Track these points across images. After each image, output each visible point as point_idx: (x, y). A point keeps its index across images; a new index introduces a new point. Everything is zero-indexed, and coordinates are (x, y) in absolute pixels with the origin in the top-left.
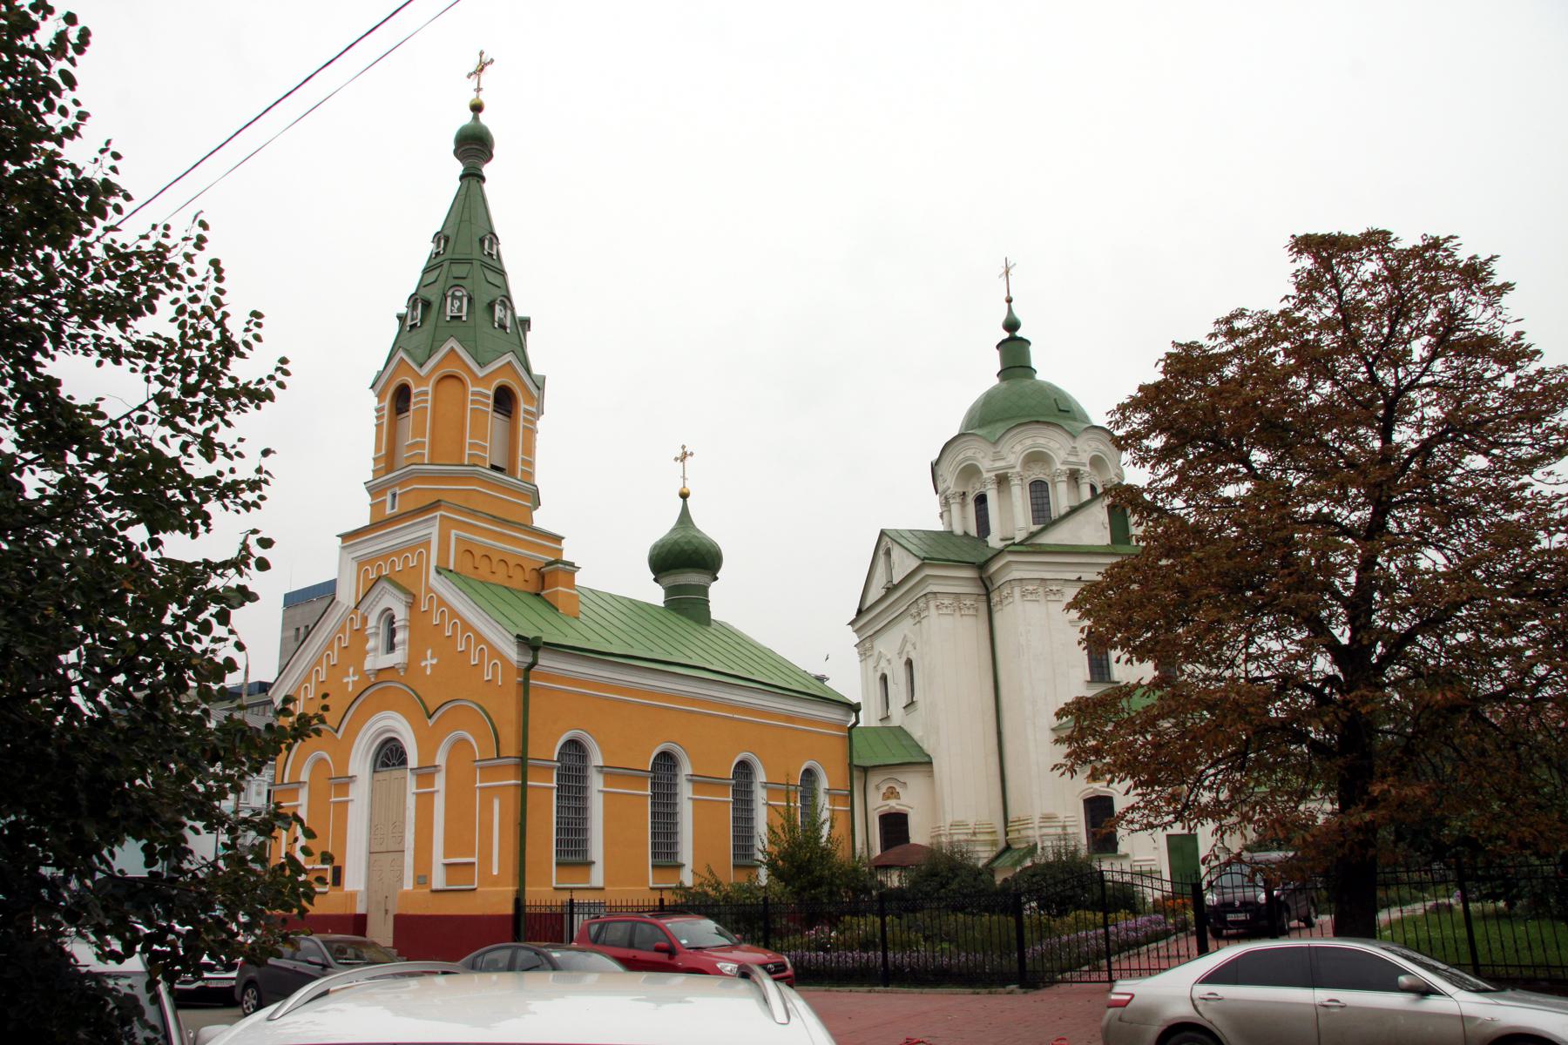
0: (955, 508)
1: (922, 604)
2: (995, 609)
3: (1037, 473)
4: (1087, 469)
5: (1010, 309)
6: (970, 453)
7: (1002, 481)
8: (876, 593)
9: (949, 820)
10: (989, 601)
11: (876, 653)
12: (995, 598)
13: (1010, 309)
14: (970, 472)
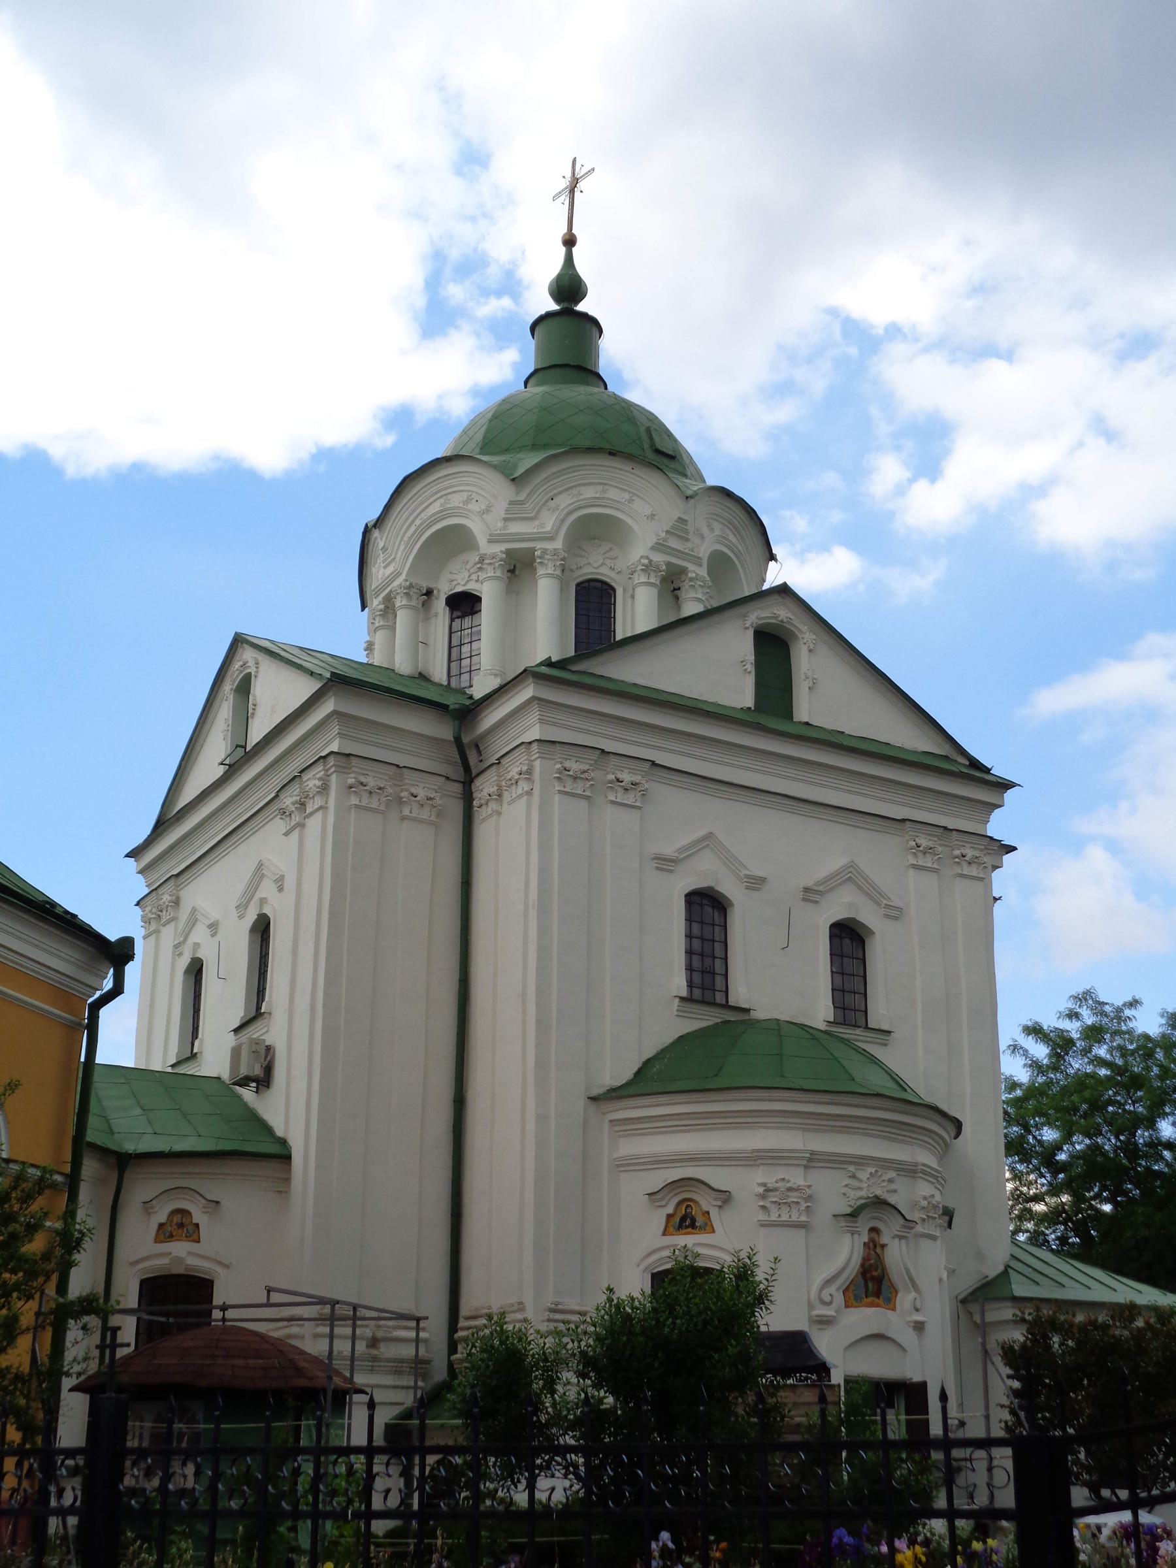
0: (403, 618)
1: (312, 781)
2: (480, 814)
4: (703, 572)
5: (569, 260)
6: (456, 500)
7: (518, 568)
8: (208, 769)
10: (468, 799)
11: (184, 914)
12: (485, 787)
13: (569, 260)
14: (449, 542)
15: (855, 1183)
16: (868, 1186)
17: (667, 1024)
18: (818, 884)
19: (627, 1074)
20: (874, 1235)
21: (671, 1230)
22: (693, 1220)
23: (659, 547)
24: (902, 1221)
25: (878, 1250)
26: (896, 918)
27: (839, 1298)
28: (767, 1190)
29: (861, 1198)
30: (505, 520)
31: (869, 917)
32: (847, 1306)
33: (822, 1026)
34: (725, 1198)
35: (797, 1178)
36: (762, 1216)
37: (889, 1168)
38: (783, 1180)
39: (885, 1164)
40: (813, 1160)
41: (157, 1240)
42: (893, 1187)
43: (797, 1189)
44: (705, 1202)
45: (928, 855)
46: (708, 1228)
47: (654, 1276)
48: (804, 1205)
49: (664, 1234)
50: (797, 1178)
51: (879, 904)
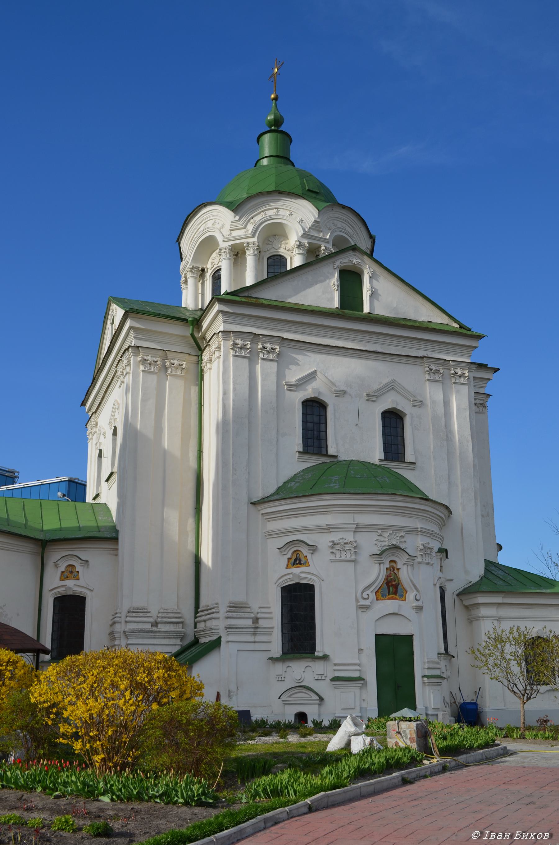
9: (126, 606)
15: (381, 539)
16: (387, 540)
18: (375, 392)
19: (272, 490)
20: (393, 564)
21: (290, 565)
22: (300, 560)
23: (305, 235)
24: (407, 557)
25: (396, 571)
26: (420, 407)
27: (373, 596)
28: (335, 544)
29: (385, 546)
30: (231, 230)
31: (403, 406)
32: (377, 599)
33: (377, 463)
34: (314, 549)
35: (350, 537)
36: (332, 557)
37: (401, 531)
38: (343, 538)
39: (396, 529)
40: (358, 528)
41: (61, 580)
42: (403, 540)
43: (350, 543)
44: (305, 551)
45: (436, 374)
46: (307, 564)
47: (282, 588)
48: (353, 550)
49: (287, 568)
50: (350, 537)
51: (410, 400)
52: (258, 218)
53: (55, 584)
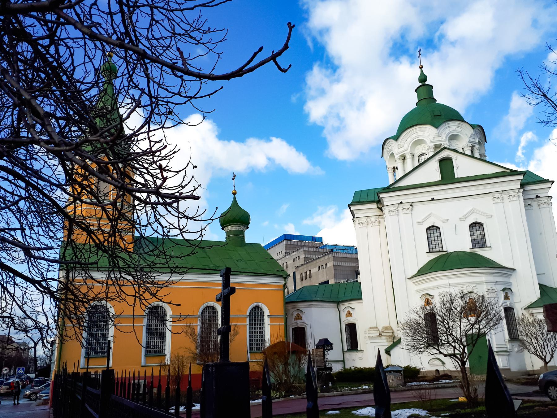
3: (419, 150)
5: (422, 72)
7: (404, 158)
13: (422, 72)
17: (425, 258)
19: (416, 272)
23: (431, 142)
52: (409, 140)
53: (346, 320)
